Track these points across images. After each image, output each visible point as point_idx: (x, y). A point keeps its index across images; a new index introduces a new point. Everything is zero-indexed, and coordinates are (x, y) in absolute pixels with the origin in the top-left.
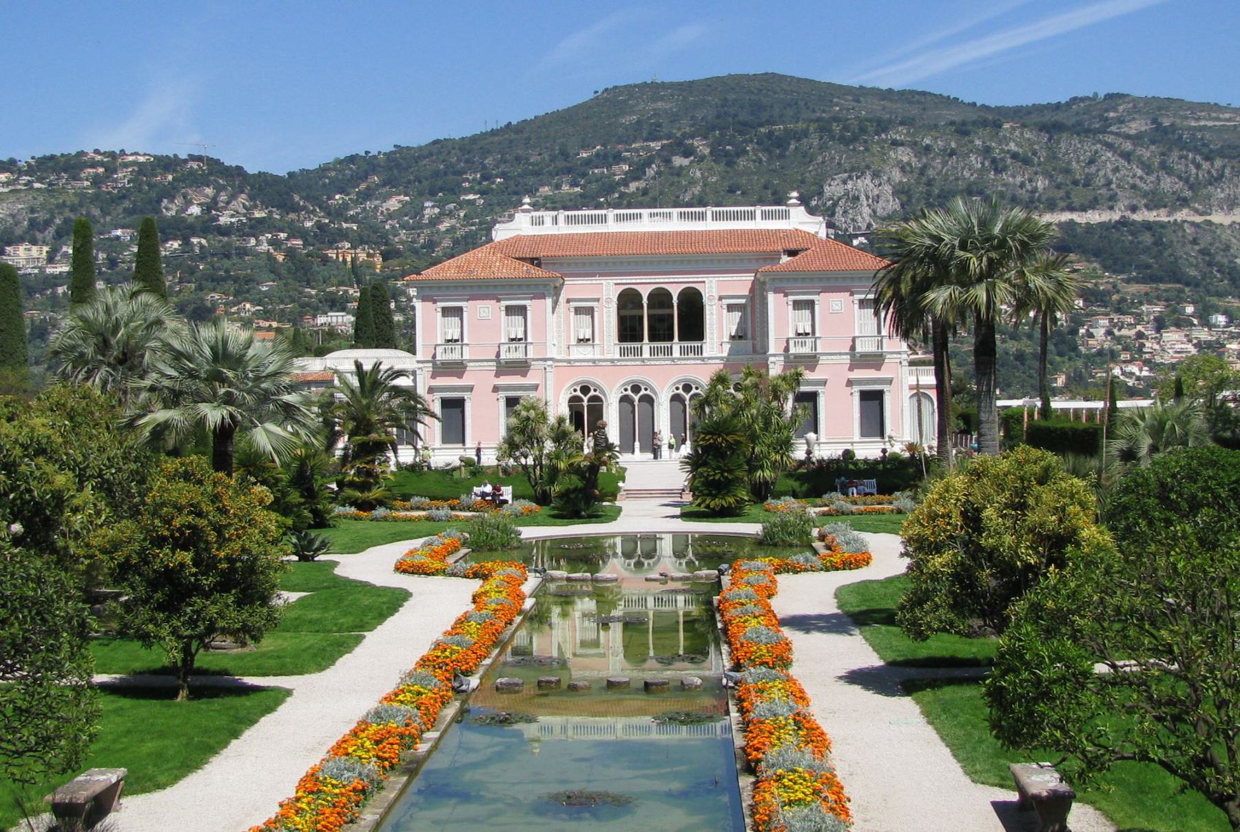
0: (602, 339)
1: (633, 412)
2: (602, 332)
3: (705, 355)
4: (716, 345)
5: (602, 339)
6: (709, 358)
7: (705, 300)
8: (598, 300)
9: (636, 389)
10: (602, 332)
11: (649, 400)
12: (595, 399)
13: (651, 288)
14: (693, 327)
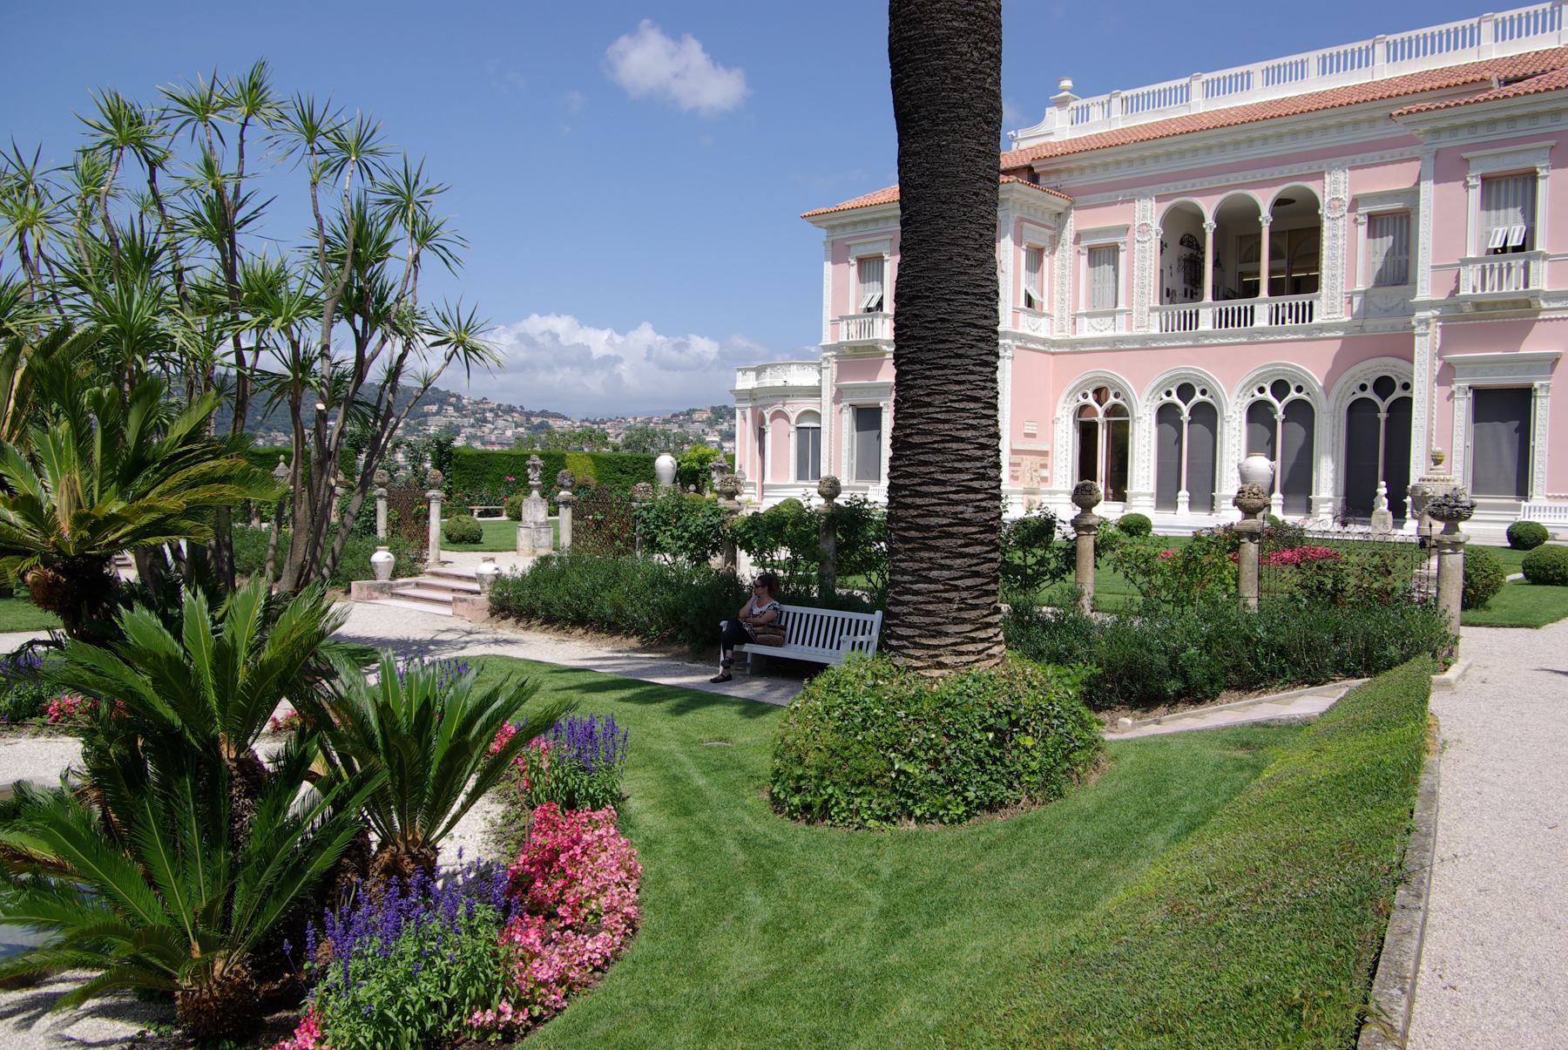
0: (1129, 301)
1: (1179, 441)
2: (1130, 287)
3: (1316, 320)
4: (1341, 301)
5: (1129, 301)
6: (1321, 328)
7: (1324, 211)
8: (1127, 229)
9: (1186, 391)
10: (1130, 287)
11: (1207, 415)
12: (1115, 410)
13: (1217, 200)
14: (1299, 270)
